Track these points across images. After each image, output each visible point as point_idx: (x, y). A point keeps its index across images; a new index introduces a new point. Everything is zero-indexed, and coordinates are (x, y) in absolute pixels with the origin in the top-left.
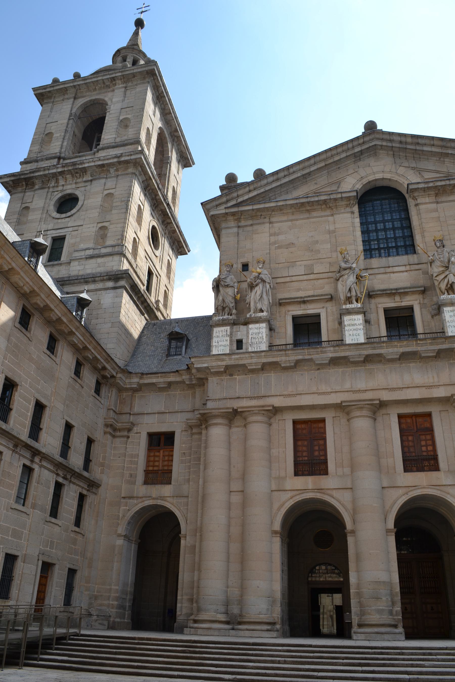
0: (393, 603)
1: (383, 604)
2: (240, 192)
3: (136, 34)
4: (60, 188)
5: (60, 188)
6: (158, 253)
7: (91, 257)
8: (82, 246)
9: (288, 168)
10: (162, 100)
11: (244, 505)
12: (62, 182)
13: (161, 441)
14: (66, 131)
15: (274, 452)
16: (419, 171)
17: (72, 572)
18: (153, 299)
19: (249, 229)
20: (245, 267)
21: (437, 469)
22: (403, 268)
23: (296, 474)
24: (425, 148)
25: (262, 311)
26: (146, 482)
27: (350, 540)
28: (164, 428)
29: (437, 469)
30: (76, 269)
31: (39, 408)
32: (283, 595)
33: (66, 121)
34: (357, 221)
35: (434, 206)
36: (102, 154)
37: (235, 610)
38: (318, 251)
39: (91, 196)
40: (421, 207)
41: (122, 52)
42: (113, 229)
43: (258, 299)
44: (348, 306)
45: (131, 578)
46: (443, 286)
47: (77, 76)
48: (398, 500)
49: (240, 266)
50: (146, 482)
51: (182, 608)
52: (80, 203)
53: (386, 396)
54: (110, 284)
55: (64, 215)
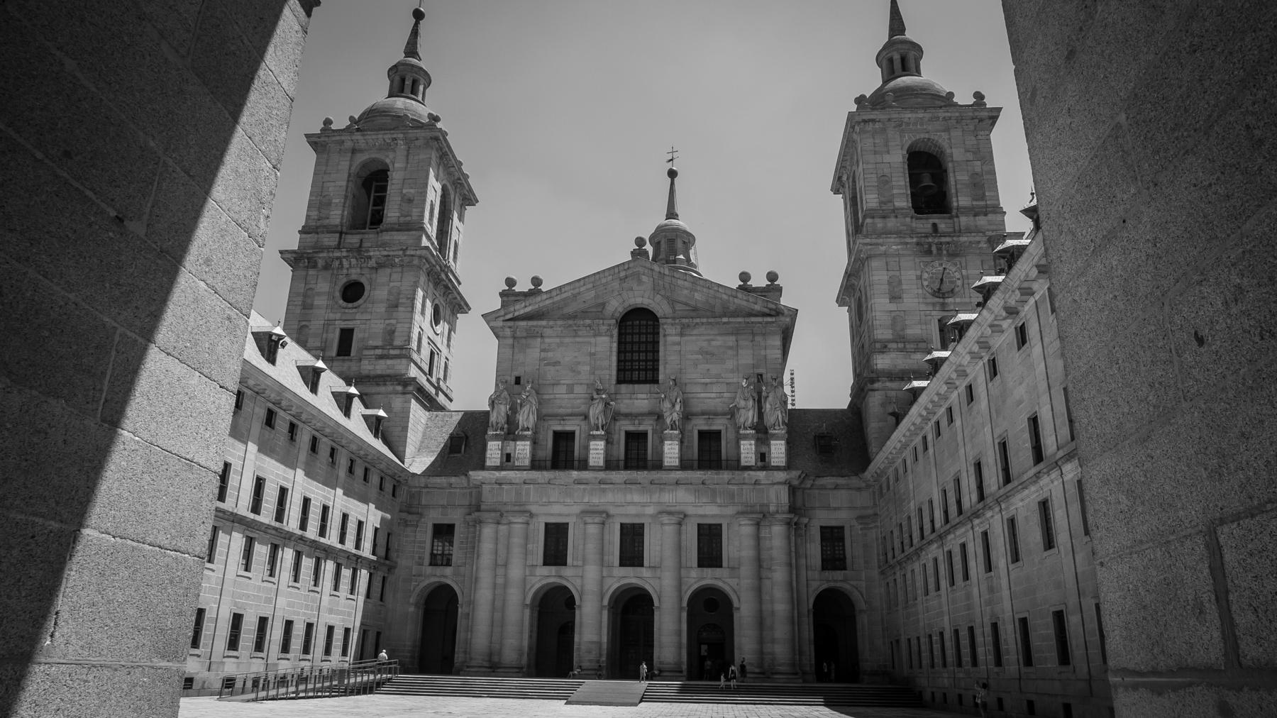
0: (601, 655)
1: (593, 656)
2: (517, 307)
3: (415, 33)
4: (345, 271)
5: (345, 271)
6: (439, 329)
7: (381, 357)
8: (371, 343)
9: (560, 288)
10: (447, 161)
11: (505, 586)
12: (345, 263)
13: (444, 532)
14: (346, 197)
15: (530, 546)
16: (672, 302)
17: (378, 634)
18: (434, 380)
19: (524, 341)
20: (518, 380)
21: (642, 565)
22: (644, 396)
23: (545, 564)
24: (680, 282)
25: (528, 429)
26: (431, 564)
27: (577, 612)
28: (446, 522)
29: (642, 565)
30: (367, 367)
31: (360, 524)
32: (530, 648)
33: (344, 183)
34: (615, 345)
35: (677, 339)
36: (386, 237)
37: (496, 659)
38: (579, 373)
39: (379, 291)
40: (669, 339)
41: (401, 68)
42: (400, 328)
43: (526, 418)
44: (595, 433)
45: (419, 635)
46: (668, 421)
47: (351, 118)
48: (613, 585)
49: (513, 379)
50: (431, 564)
51: (459, 657)
52: (366, 293)
53: (612, 511)
54: (400, 388)
55: (350, 305)
